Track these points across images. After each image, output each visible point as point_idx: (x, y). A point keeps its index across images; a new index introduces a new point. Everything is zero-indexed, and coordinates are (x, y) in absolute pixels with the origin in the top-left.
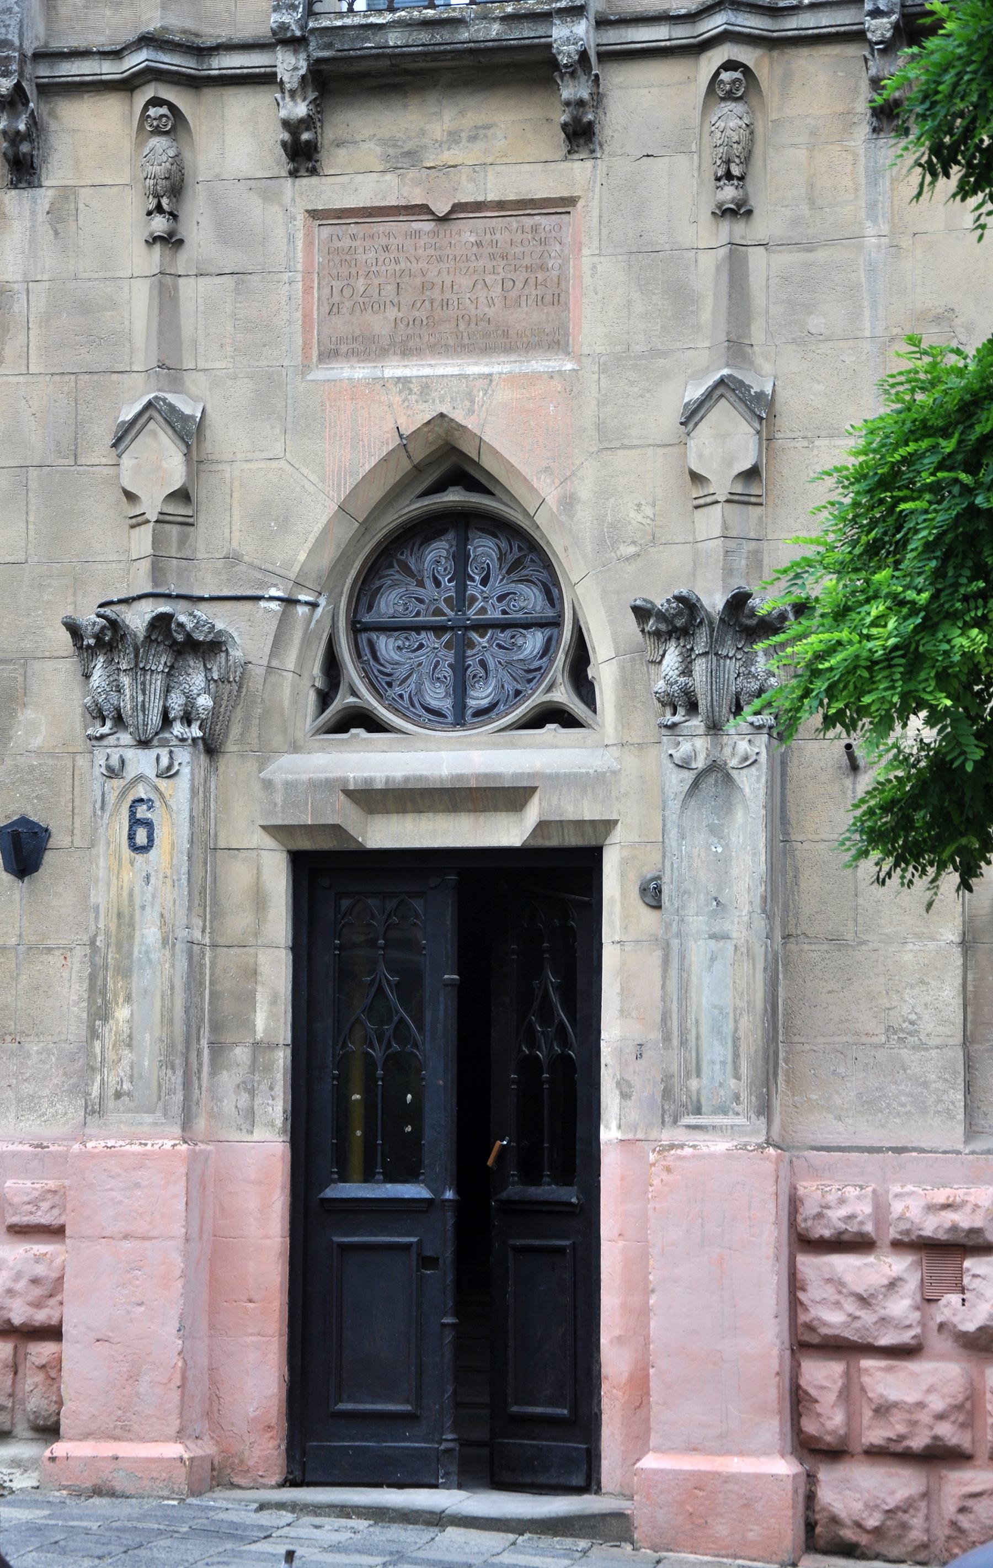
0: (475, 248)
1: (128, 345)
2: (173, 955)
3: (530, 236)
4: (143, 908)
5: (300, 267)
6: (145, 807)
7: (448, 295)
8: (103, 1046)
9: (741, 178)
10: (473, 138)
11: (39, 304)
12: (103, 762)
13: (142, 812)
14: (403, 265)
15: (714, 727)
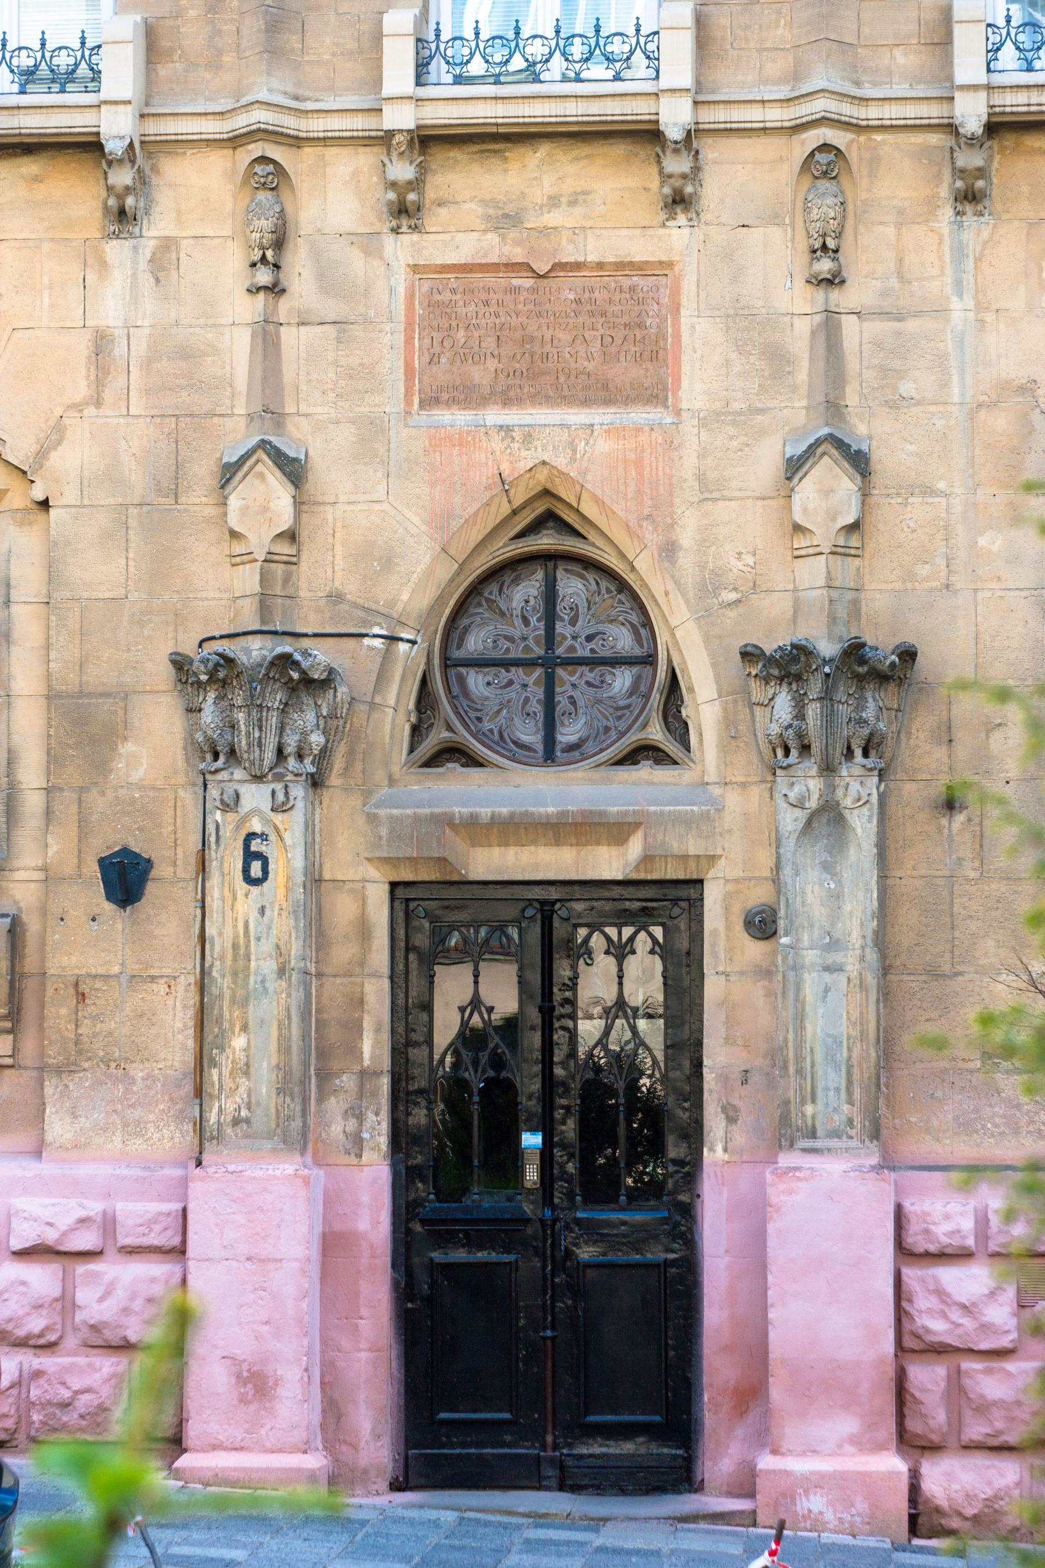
0: (574, 305)
1: (229, 389)
2: (290, 985)
3: (628, 296)
4: (258, 939)
5: (403, 319)
6: (259, 840)
7: (548, 348)
8: (220, 1074)
9: (836, 251)
10: (573, 203)
11: (140, 347)
12: (217, 796)
13: (255, 846)
14: (503, 319)
15: (828, 769)
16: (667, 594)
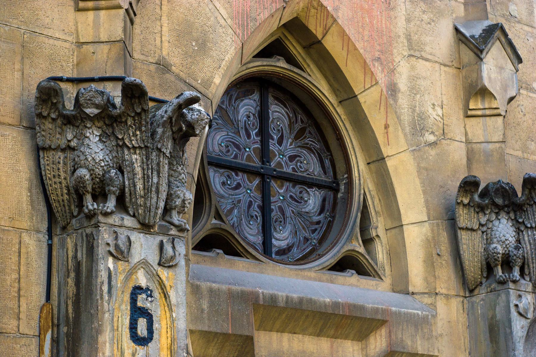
6: (144, 296)
16: (386, 127)
